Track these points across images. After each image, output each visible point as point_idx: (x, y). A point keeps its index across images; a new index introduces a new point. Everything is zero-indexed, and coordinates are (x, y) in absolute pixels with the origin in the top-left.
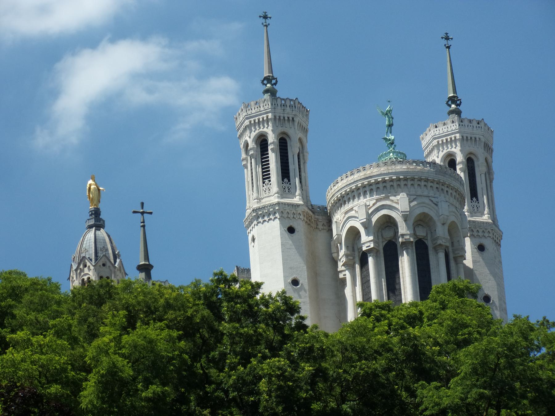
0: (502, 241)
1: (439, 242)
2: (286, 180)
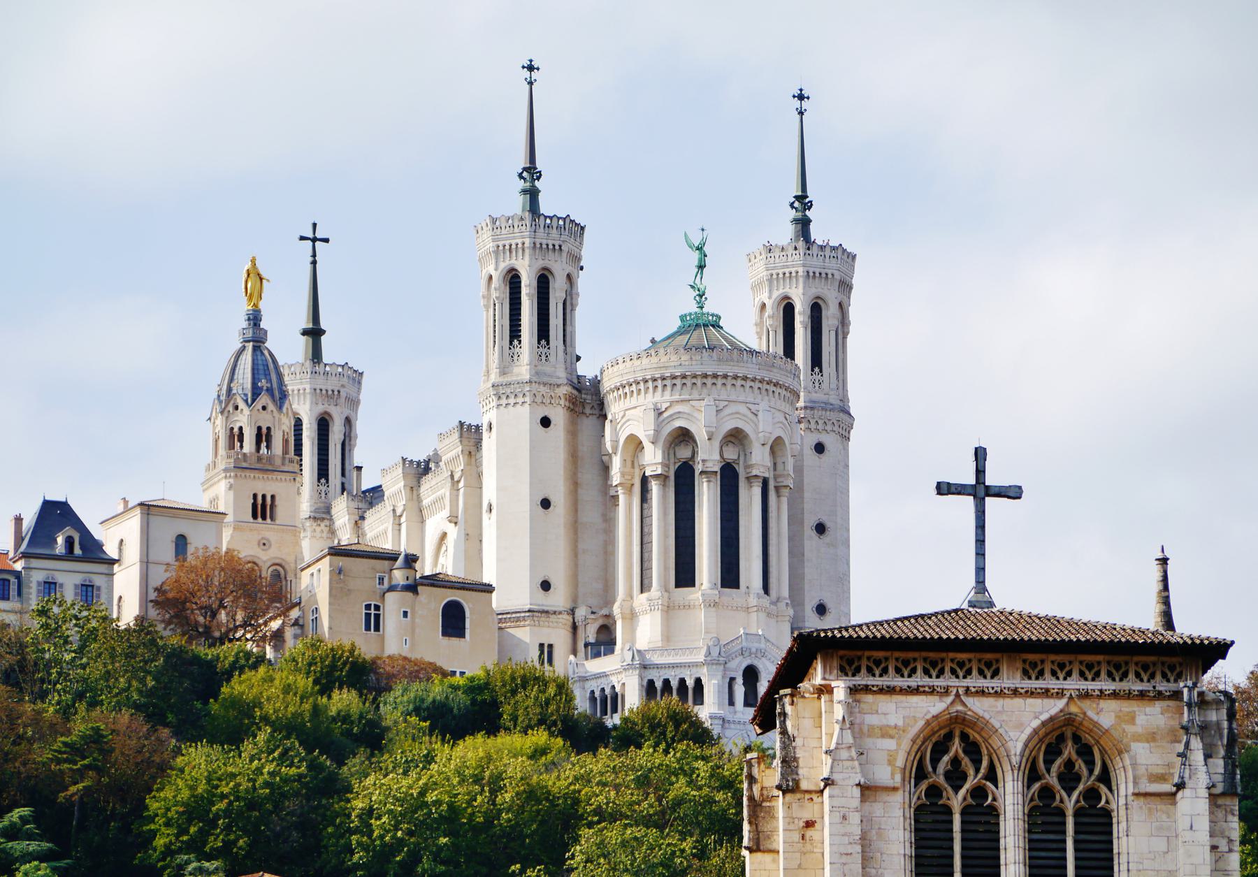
0: (852, 432)
1: (755, 472)
2: (543, 342)
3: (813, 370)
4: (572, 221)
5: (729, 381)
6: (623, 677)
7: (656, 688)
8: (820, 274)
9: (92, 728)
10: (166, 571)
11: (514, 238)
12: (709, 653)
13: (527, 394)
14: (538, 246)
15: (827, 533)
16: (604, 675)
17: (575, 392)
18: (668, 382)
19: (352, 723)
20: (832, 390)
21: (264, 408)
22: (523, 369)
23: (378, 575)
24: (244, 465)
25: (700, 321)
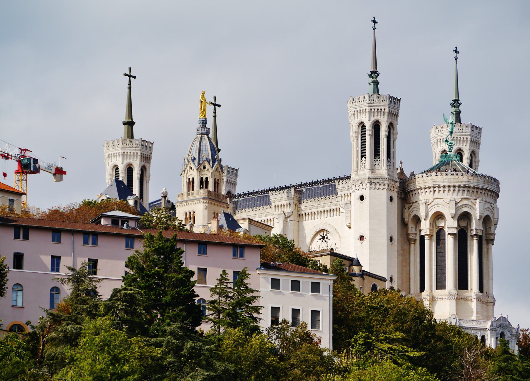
18: (461, 189)
24: (211, 197)
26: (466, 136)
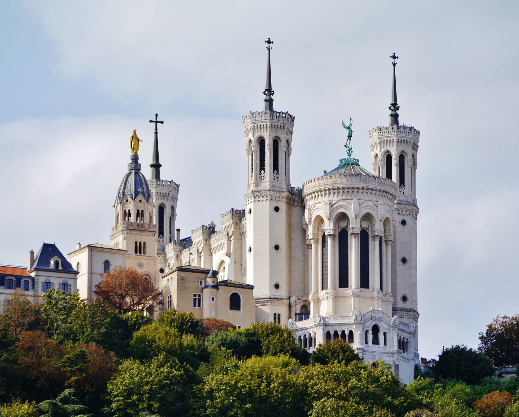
1: (376, 234)
2: (276, 171)
3: (400, 186)
4: (289, 115)
5: (365, 191)
6: (315, 330)
7: (331, 335)
8: (404, 140)
9: (81, 351)
10: (101, 277)
11: (262, 122)
12: (356, 319)
13: (268, 196)
14: (273, 126)
15: (407, 263)
16: (305, 329)
17: (290, 195)
18: (336, 191)
19: (195, 350)
20: (410, 195)
21: (140, 201)
22: (266, 184)
23: (200, 280)
24: (131, 228)
25: (349, 162)
26: (392, 138)
